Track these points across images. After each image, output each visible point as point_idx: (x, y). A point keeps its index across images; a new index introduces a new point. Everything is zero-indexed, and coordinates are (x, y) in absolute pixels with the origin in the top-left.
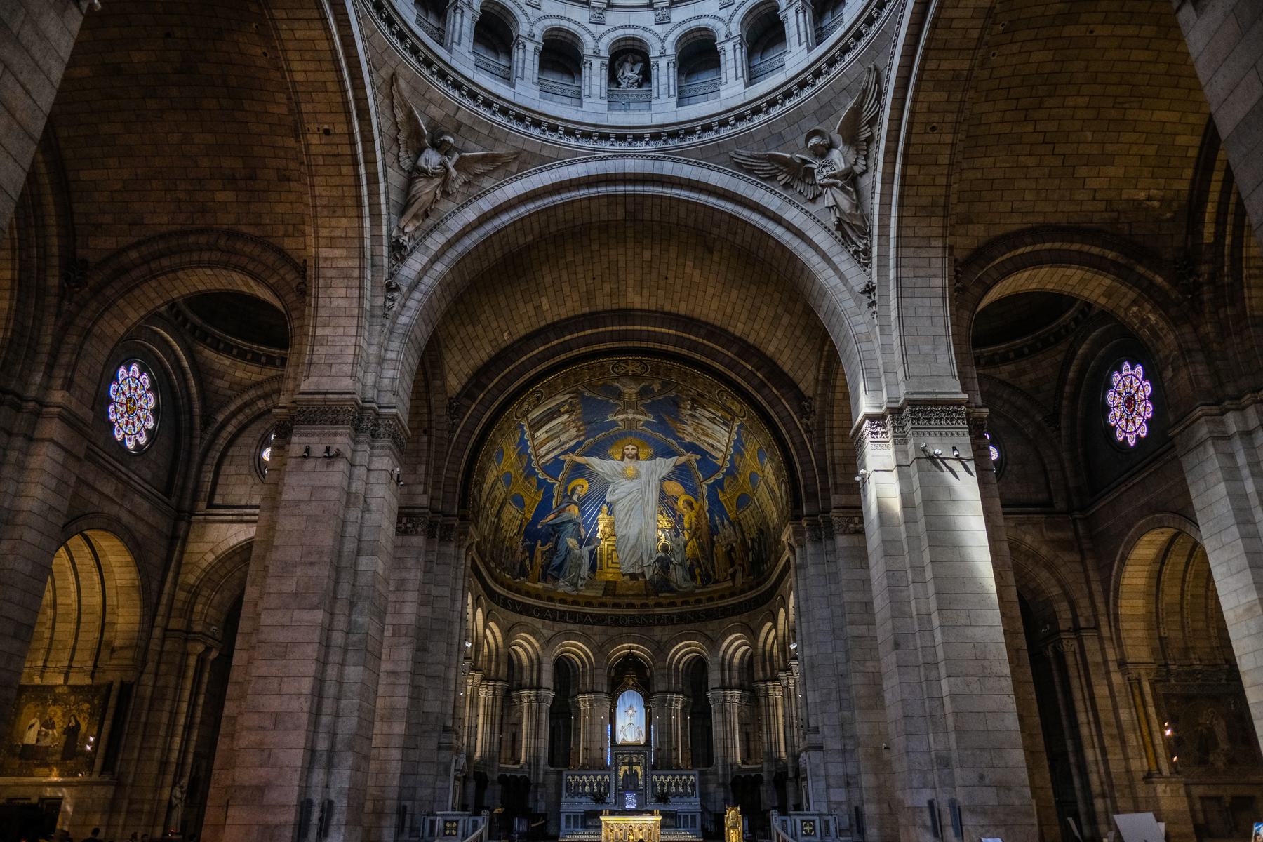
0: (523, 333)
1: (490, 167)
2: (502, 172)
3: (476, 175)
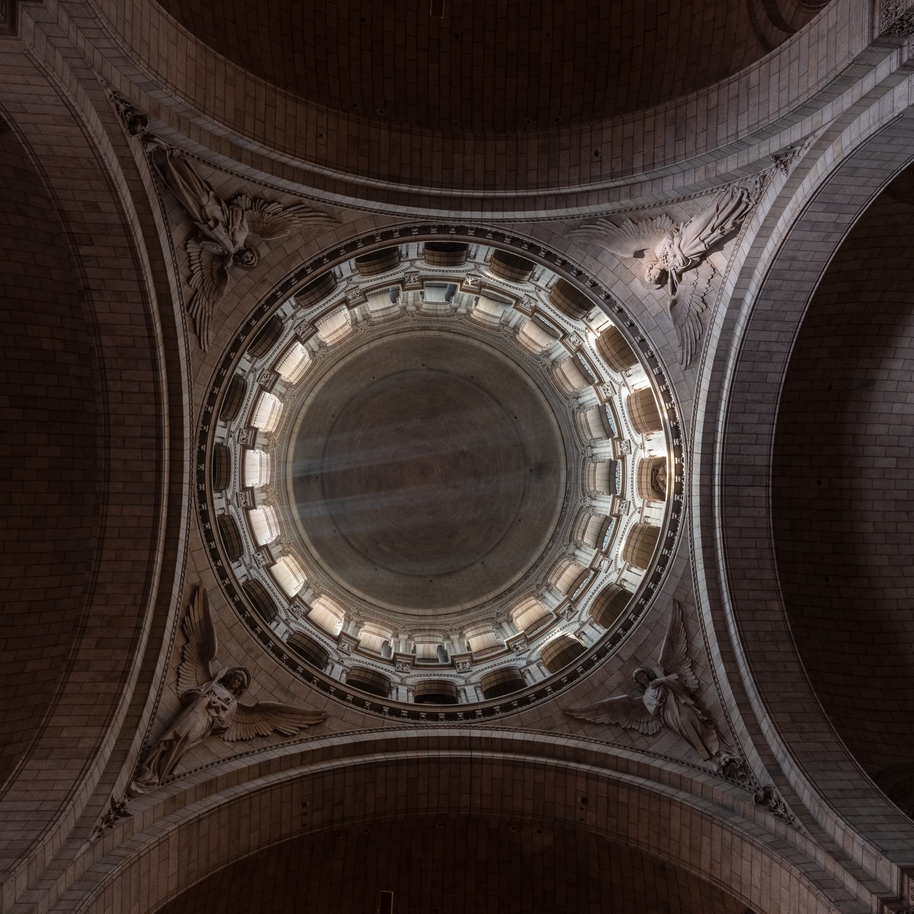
1: (683, 635)
2: (691, 623)
3: (688, 653)
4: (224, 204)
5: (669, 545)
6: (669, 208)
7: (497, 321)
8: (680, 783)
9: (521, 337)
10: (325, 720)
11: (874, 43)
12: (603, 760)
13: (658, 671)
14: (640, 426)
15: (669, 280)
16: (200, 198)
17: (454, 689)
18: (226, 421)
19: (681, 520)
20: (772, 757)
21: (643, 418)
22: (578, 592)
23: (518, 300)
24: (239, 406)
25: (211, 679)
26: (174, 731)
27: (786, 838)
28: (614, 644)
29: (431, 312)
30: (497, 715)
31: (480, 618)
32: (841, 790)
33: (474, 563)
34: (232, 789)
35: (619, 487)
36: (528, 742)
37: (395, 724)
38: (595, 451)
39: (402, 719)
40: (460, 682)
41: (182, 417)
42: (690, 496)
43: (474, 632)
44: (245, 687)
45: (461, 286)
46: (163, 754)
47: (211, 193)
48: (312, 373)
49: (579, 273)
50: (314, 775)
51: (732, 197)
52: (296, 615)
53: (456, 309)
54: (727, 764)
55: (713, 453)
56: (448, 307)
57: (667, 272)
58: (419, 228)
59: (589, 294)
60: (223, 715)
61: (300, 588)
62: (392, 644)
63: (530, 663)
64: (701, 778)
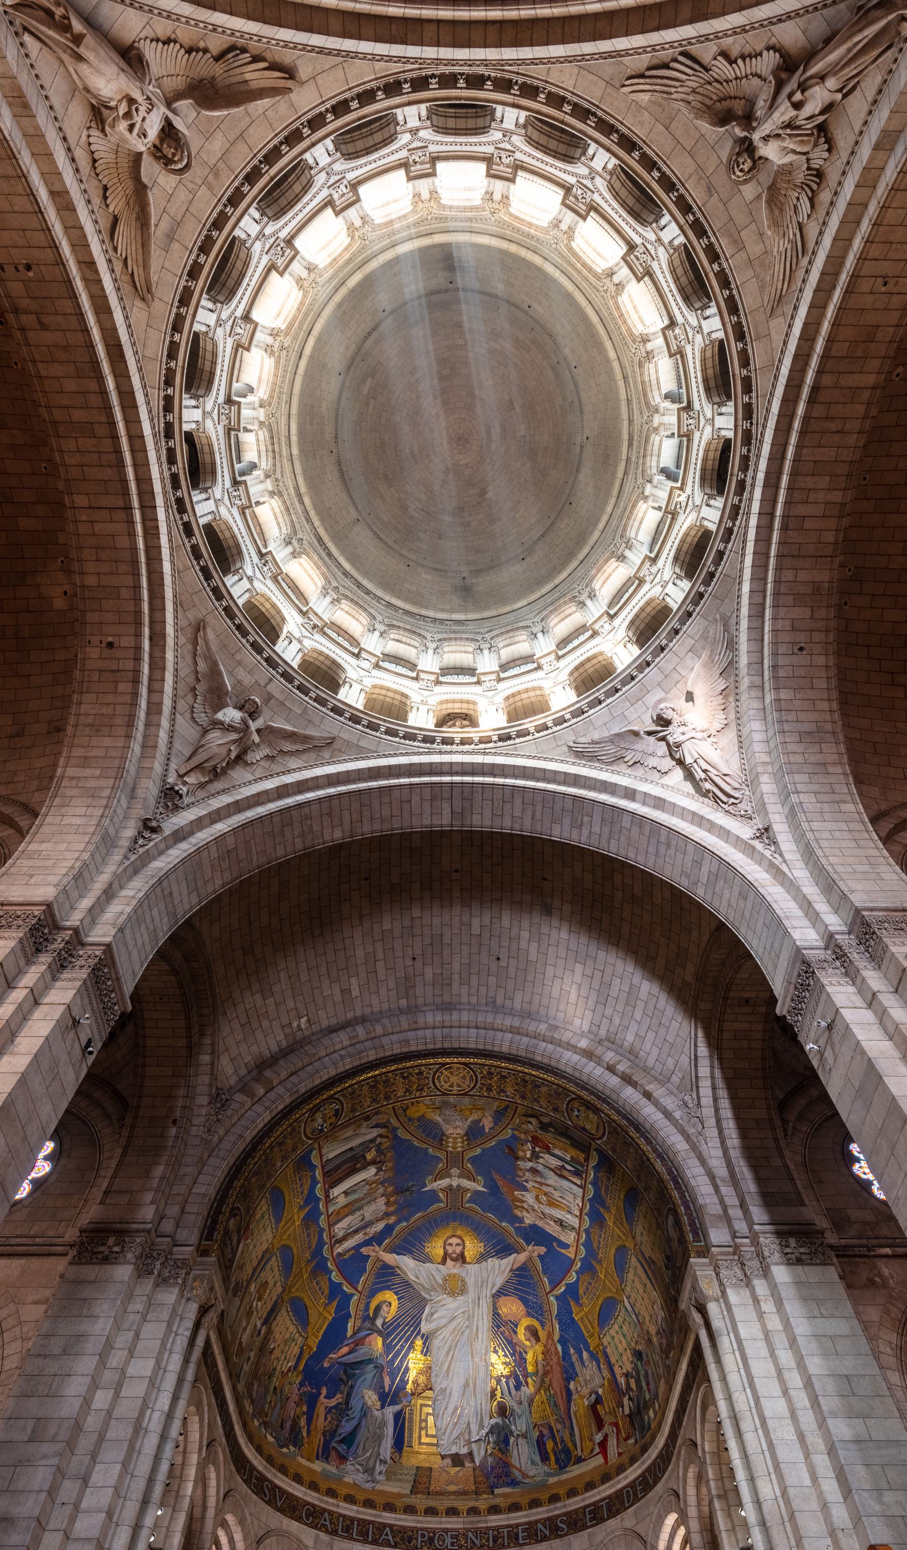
0: (325, 1024)
4: (821, 119)
5: (390, 732)
6: (733, 726)
7: (633, 535)
8: (149, 746)
9: (613, 563)
10: (143, 299)
11: (858, 911)
12: (158, 665)
13: (259, 723)
14: (511, 700)
15: (659, 728)
16: (835, 74)
17: (208, 484)
18: (525, 126)
19: (416, 744)
20: (192, 833)
21: (519, 704)
22: (334, 635)
23: (654, 560)
24: (546, 150)
25: (169, 105)
26: (84, 35)
27: (116, 847)
28: (282, 675)
29: (650, 448)
30: (186, 541)
31: (294, 518)
32: (171, 894)
33: (357, 508)
34: (24, 143)
35: (448, 679)
36: (162, 579)
37: (154, 403)
38: (486, 652)
39: (162, 414)
40: (218, 492)
41: (531, 45)
42: (441, 753)
43: (277, 510)
44: (166, 165)
45: (677, 488)
46: (49, 13)
47: (839, 96)
48: (585, 272)
49: (677, 632)
50: (69, 283)
51: (736, 789)
52: (272, 251)
53: (650, 481)
54: (177, 792)
55: (484, 774)
56: (654, 471)
57: (667, 726)
58: (750, 430)
59: (654, 643)
60: (123, 126)
61: (307, 257)
62: (251, 398)
63: (250, 579)
64: (158, 767)
